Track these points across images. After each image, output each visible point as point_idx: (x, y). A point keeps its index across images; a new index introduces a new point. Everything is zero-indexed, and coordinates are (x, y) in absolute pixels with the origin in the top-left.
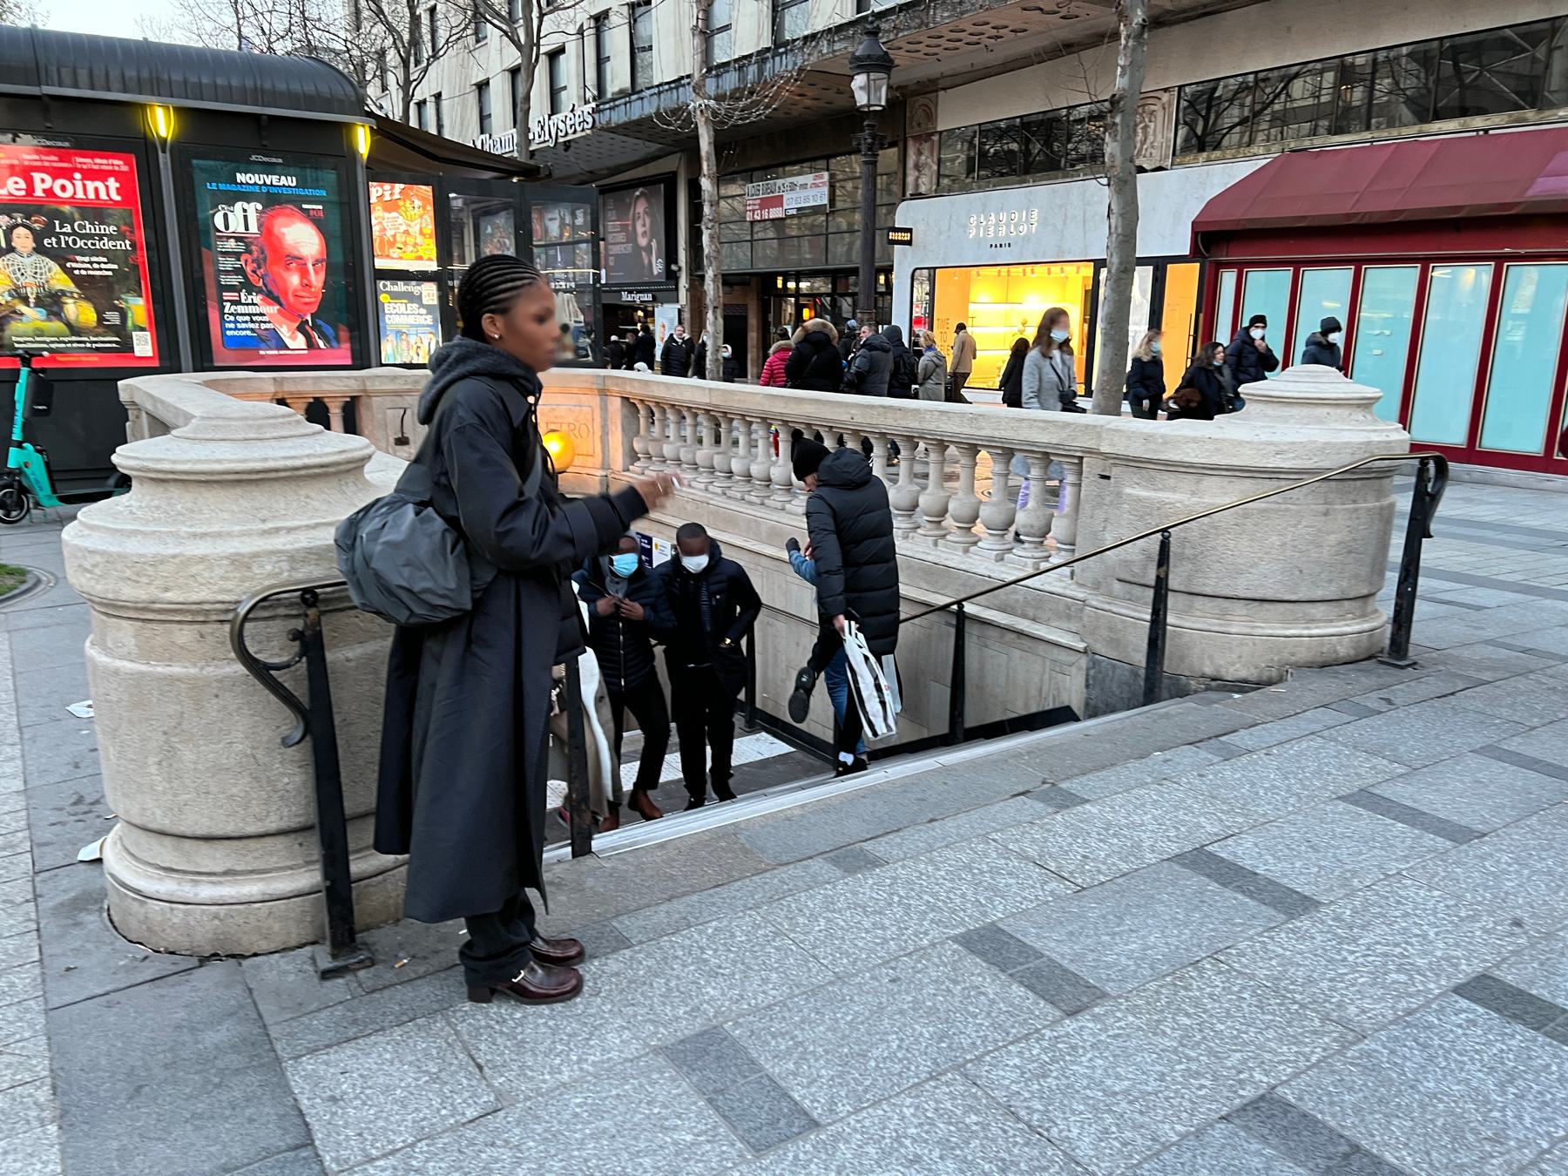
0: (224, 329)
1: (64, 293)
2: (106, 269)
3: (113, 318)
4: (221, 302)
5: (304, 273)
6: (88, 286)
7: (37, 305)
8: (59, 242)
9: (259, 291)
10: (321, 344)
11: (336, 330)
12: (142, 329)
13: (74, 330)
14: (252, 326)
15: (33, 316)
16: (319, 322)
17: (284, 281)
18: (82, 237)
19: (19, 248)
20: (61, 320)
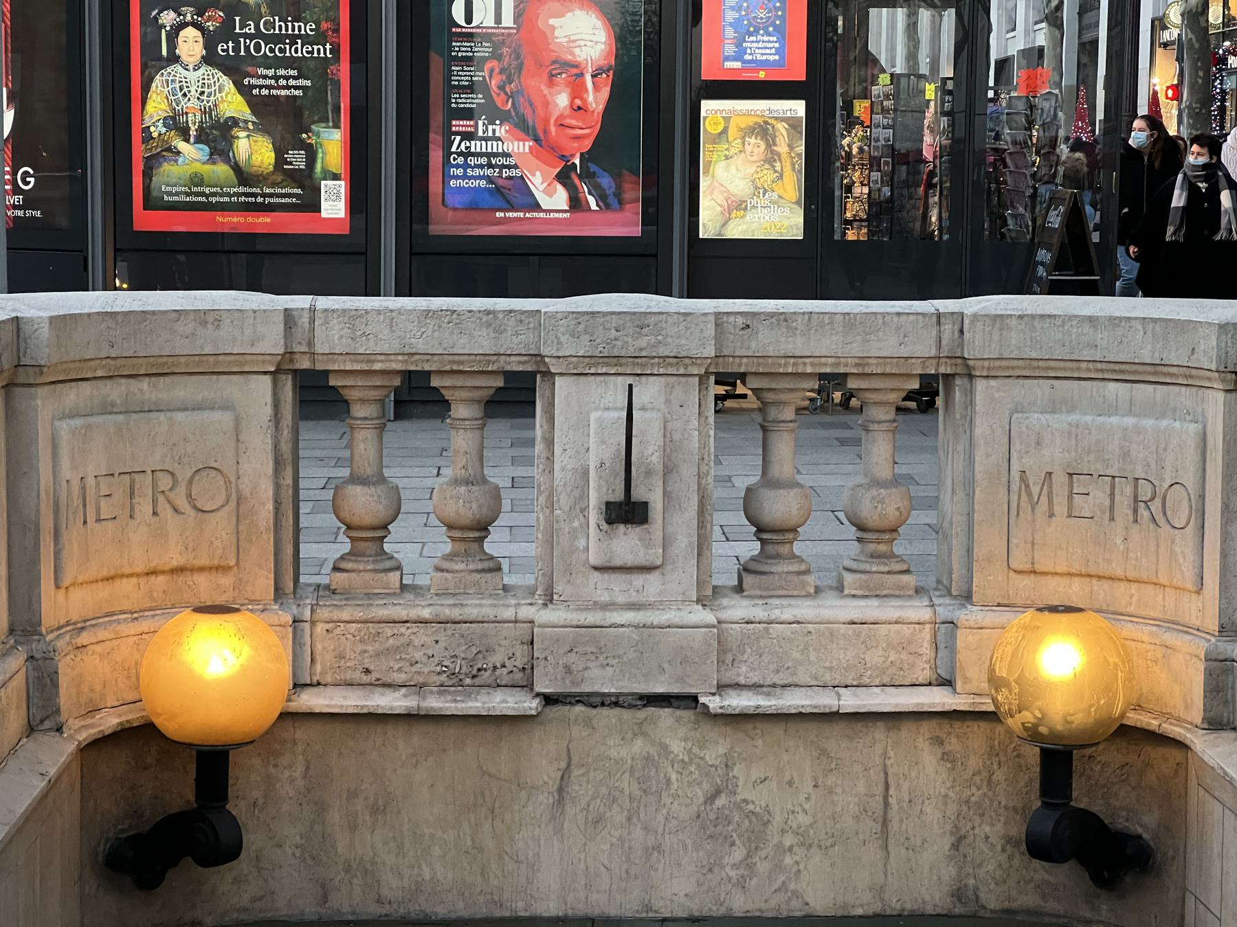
0: (446, 177)
1: (234, 122)
2: (291, 86)
3: (297, 159)
4: (448, 135)
5: (577, 90)
6: (267, 111)
7: (198, 140)
8: (237, 49)
9: (504, 117)
10: (592, 201)
11: (617, 178)
12: (336, 177)
13: (243, 176)
14: (489, 172)
15: (191, 154)
16: (593, 168)
17: (546, 104)
18: (268, 39)
19: (184, 58)
20: (227, 160)
